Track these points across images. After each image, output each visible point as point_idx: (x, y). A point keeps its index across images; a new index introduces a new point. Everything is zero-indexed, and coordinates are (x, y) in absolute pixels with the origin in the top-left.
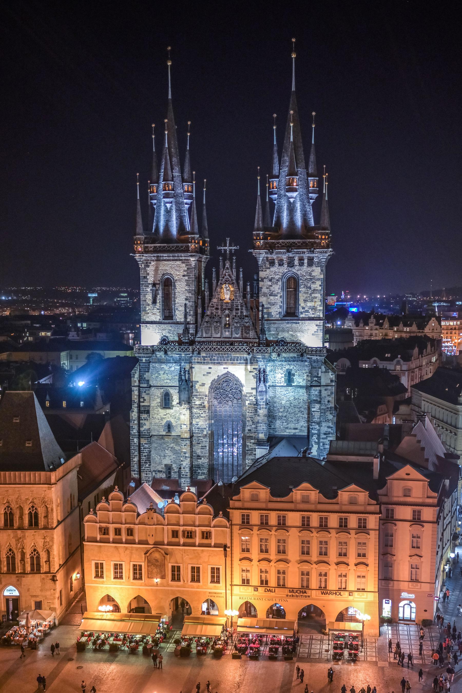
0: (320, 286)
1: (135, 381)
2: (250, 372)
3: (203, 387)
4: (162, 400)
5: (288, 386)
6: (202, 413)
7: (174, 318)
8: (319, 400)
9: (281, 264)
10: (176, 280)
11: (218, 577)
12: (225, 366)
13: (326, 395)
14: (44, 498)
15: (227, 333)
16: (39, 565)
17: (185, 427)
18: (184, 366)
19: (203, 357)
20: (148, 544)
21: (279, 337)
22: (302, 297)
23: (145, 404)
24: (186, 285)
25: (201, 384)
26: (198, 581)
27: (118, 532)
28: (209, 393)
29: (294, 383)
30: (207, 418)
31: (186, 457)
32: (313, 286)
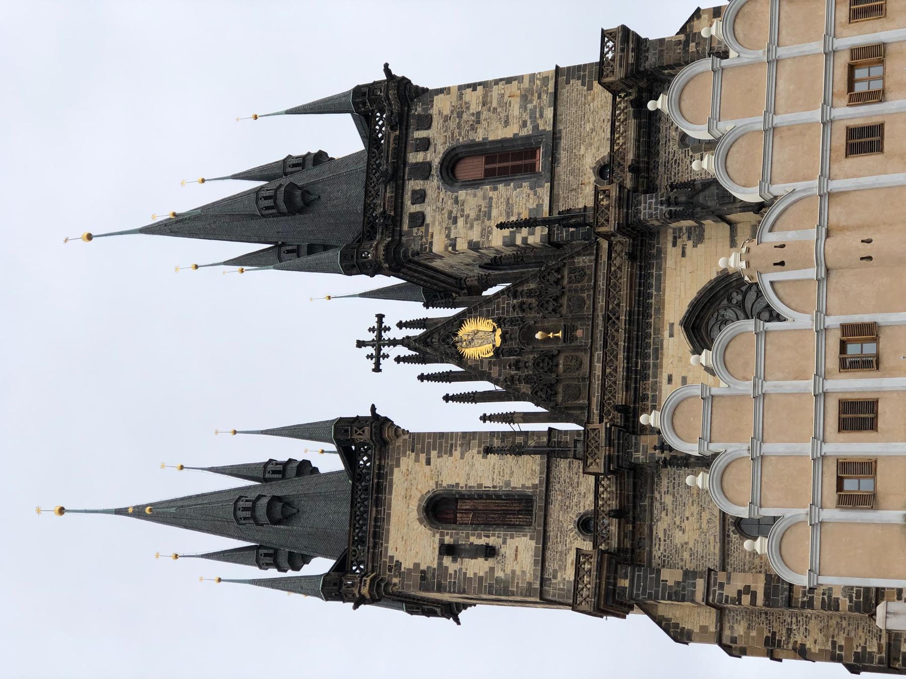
1: (704, 629)
2: (683, 254)
7: (529, 492)
9: (420, 197)
10: (437, 483)
12: (666, 333)
15: (579, 333)
18: (645, 452)
19: (635, 403)
21: (593, 179)
22: (498, 132)
23: (760, 588)
24: (451, 455)
27: (859, 416)
32: (474, 108)
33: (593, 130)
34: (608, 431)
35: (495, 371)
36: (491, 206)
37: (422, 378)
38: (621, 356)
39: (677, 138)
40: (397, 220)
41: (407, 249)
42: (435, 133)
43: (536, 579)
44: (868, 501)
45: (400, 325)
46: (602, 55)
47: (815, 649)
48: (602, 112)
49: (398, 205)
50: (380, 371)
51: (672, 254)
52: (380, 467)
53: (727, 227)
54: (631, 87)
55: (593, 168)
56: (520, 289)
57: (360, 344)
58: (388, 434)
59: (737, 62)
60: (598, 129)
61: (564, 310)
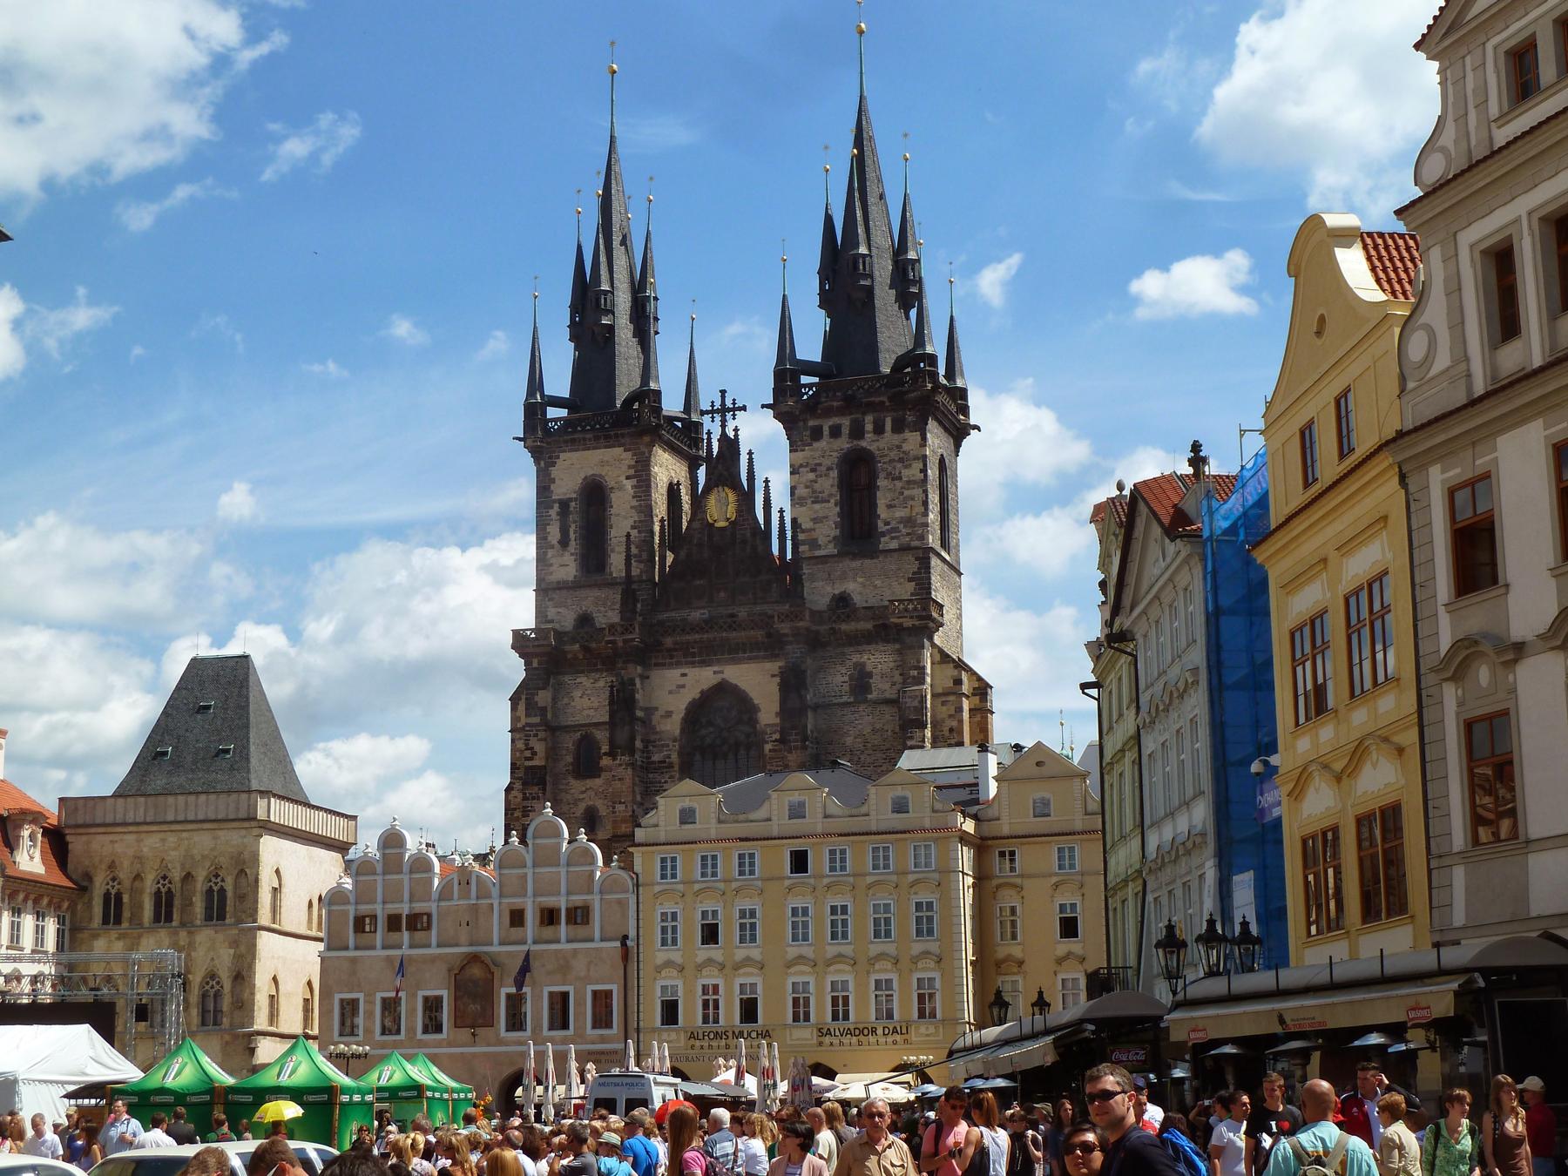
4: (577, 758)
5: (857, 703)
9: (835, 432)
13: (945, 716)
14: (241, 853)
15: (722, 594)
16: (217, 1011)
17: (622, 807)
19: (669, 650)
20: (457, 945)
22: (882, 501)
23: (536, 762)
26: (565, 1026)
27: (394, 923)
32: (906, 473)
38: (697, 636)
42: (889, 436)
45: (736, 430)
47: (511, 797)
49: (829, 412)
51: (774, 666)
52: (623, 435)
57: (723, 392)
58: (647, 439)
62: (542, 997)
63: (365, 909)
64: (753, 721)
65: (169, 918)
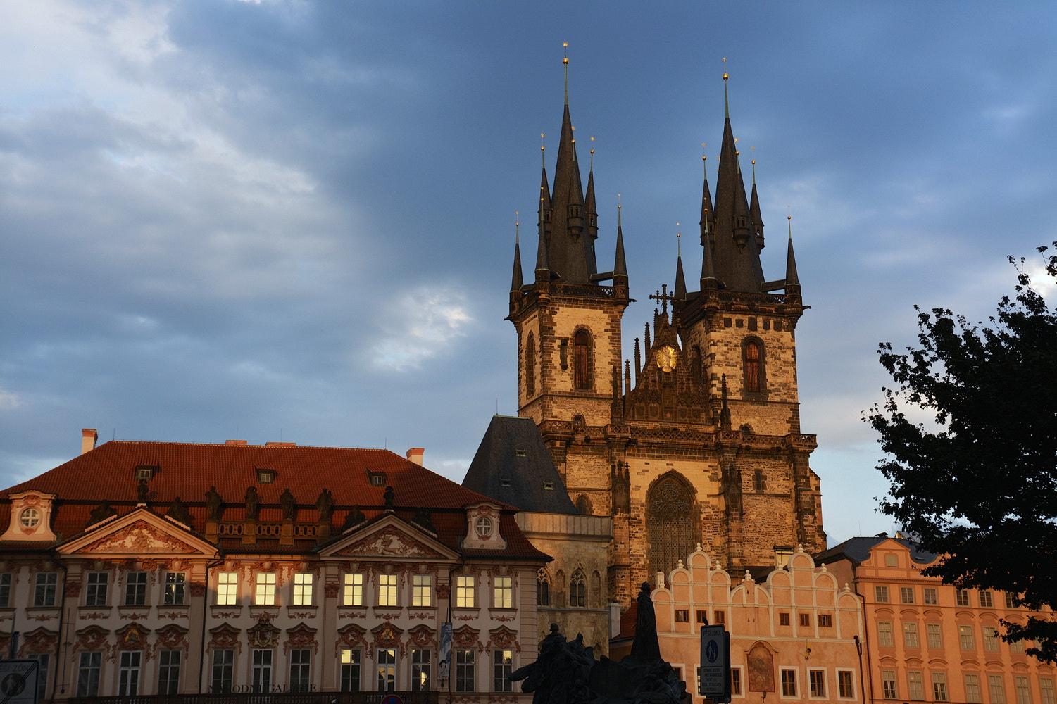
0: (792, 356)
2: (705, 471)
3: (638, 492)
6: (636, 532)
8: (812, 509)
9: (739, 324)
11: (850, 687)
12: (668, 462)
14: (594, 559)
15: (669, 415)
17: (622, 547)
20: (747, 634)
21: (743, 424)
22: (769, 371)
24: (610, 344)
25: (634, 487)
28: (646, 501)
29: (766, 489)
30: (644, 539)
31: (624, 595)
32: (782, 356)
33: (766, 423)
34: (627, 437)
35: (650, 368)
36: (733, 366)
37: (647, 325)
38: (659, 440)
39: (760, 468)
40: (729, 311)
41: (712, 317)
43: (553, 392)
44: (678, 619)
46: (804, 435)
48: (775, 428)
50: (650, 298)
51: (705, 465)
52: (603, 302)
53: (717, 493)
54: (787, 447)
55: (748, 424)
56: (691, 382)
57: (664, 286)
58: (621, 307)
59: (813, 576)
60: (767, 426)
61: (680, 406)
62: (806, 674)
63: (682, 606)
64: (694, 499)
65: (547, 602)
